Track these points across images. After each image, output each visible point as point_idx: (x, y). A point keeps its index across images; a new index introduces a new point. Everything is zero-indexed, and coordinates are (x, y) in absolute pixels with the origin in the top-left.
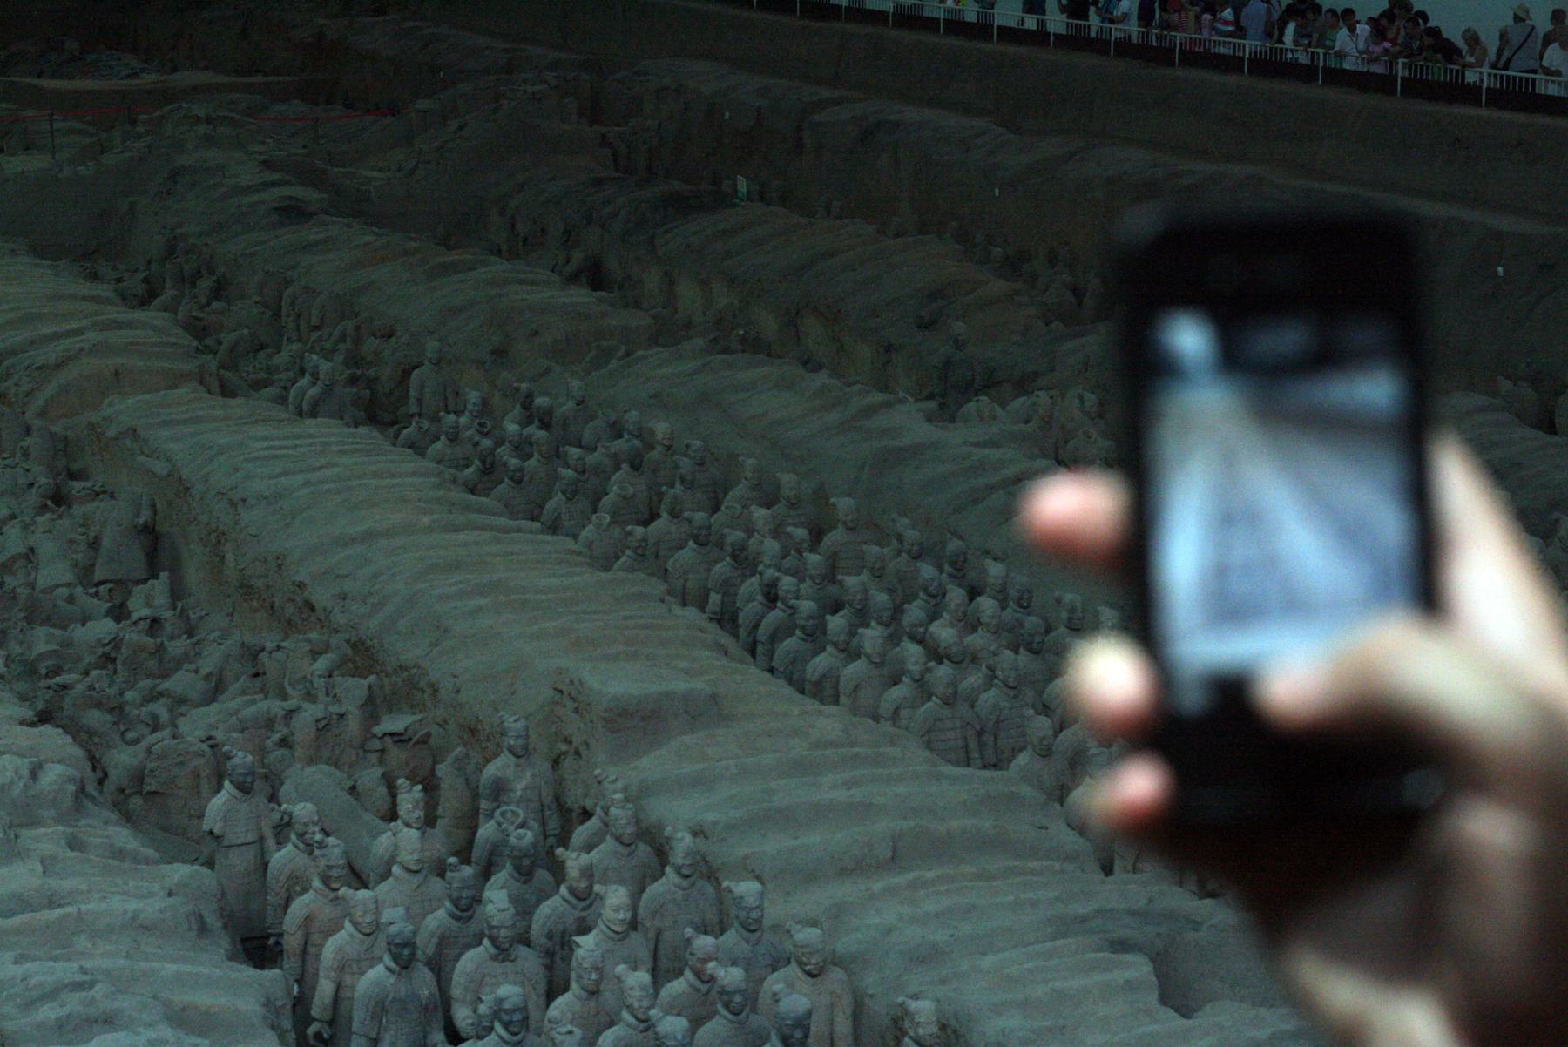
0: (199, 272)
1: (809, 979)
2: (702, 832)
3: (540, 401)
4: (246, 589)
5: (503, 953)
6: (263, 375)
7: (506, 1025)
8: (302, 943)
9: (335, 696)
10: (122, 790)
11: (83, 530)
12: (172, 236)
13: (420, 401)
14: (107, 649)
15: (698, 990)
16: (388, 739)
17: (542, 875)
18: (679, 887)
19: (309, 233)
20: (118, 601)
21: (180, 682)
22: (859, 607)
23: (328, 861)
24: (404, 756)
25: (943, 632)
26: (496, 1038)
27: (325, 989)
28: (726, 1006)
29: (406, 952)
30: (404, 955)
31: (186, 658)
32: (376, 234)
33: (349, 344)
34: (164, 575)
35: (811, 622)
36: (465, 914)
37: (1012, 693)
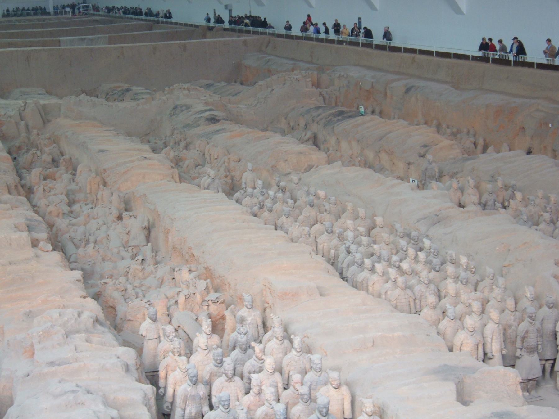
0: (181, 140)
1: (335, 389)
2: (307, 336)
3: (282, 184)
4: (174, 248)
5: (230, 379)
6: (197, 175)
7: (223, 406)
8: (165, 374)
9: (195, 286)
10: (122, 319)
11: (124, 229)
12: (173, 128)
13: (245, 184)
14: (128, 269)
15: (295, 393)
16: (210, 302)
17: (250, 351)
18: (296, 355)
19: (217, 127)
20: (135, 252)
21: (150, 281)
22: (379, 255)
23: (174, 345)
24: (216, 307)
25: (405, 265)
26: (220, 411)
27: (170, 391)
28: (302, 399)
29: (194, 379)
30: (195, 380)
31: (152, 272)
32: (239, 127)
33: (226, 164)
34: (150, 244)
35: (360, 261)
36: (219, 365)
37: (427, 286)
